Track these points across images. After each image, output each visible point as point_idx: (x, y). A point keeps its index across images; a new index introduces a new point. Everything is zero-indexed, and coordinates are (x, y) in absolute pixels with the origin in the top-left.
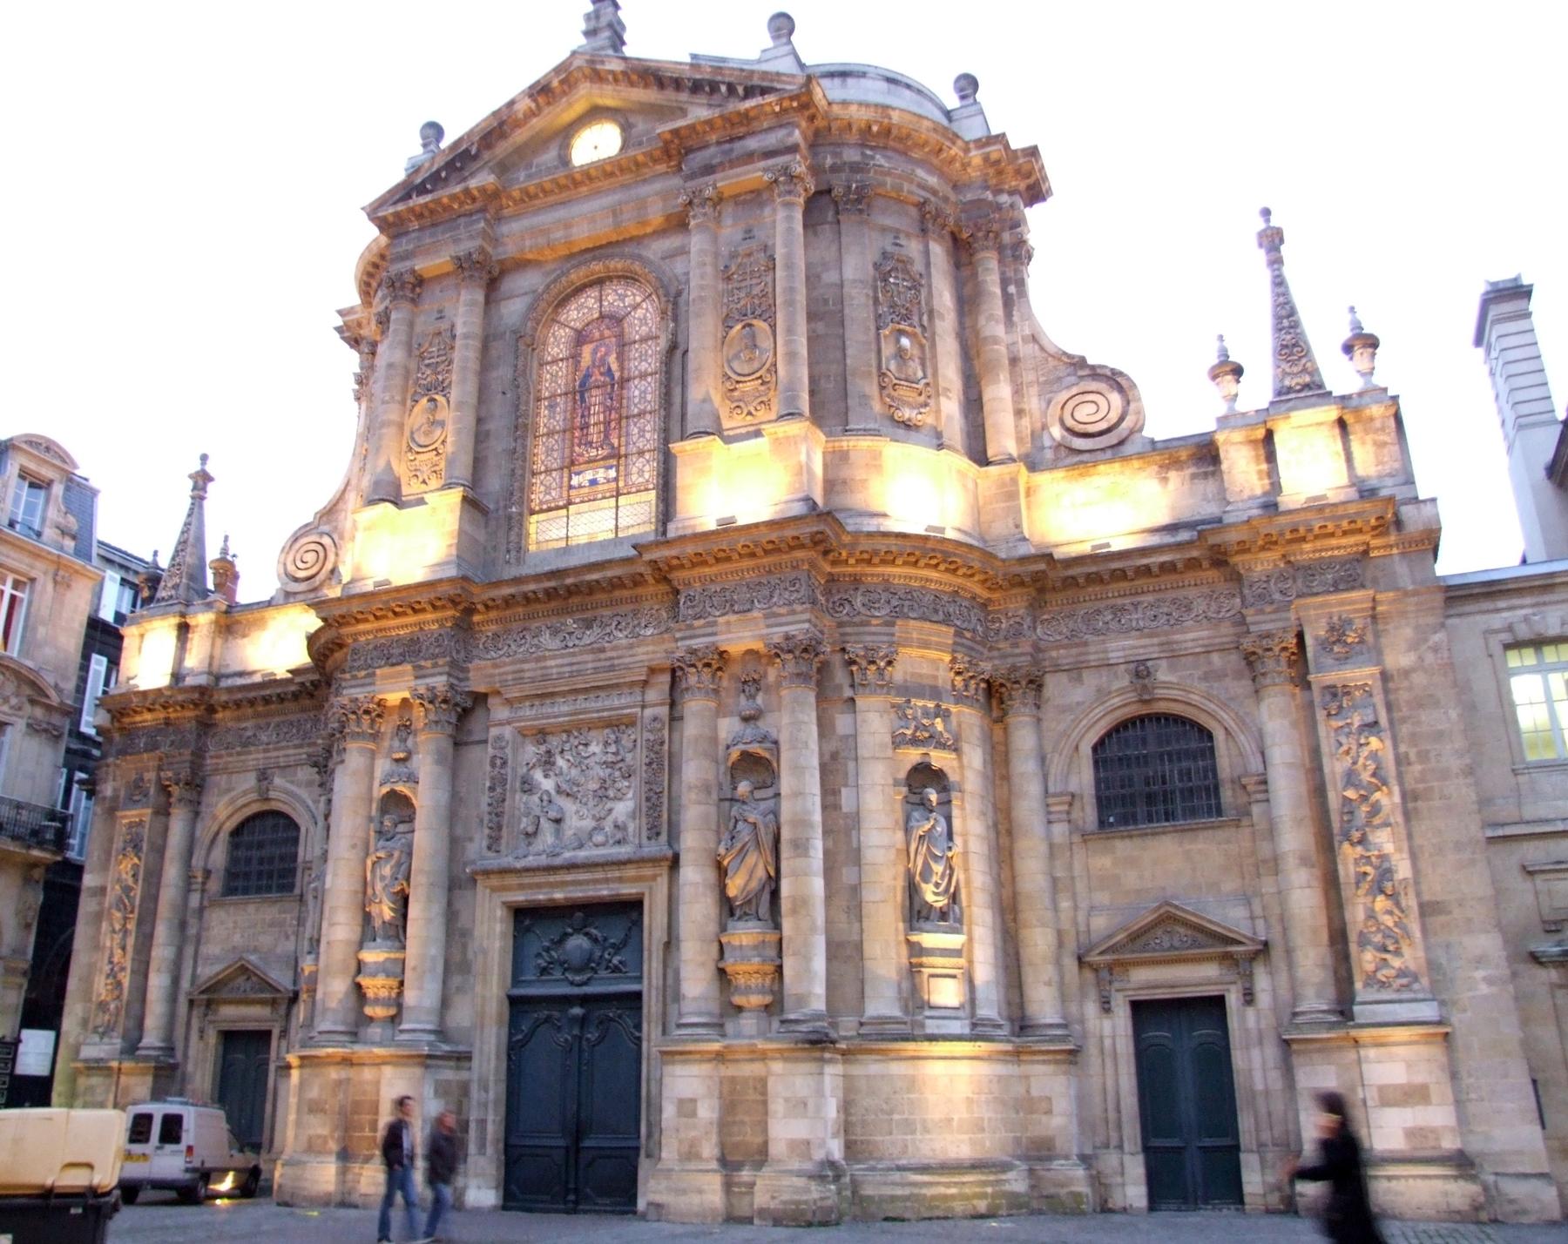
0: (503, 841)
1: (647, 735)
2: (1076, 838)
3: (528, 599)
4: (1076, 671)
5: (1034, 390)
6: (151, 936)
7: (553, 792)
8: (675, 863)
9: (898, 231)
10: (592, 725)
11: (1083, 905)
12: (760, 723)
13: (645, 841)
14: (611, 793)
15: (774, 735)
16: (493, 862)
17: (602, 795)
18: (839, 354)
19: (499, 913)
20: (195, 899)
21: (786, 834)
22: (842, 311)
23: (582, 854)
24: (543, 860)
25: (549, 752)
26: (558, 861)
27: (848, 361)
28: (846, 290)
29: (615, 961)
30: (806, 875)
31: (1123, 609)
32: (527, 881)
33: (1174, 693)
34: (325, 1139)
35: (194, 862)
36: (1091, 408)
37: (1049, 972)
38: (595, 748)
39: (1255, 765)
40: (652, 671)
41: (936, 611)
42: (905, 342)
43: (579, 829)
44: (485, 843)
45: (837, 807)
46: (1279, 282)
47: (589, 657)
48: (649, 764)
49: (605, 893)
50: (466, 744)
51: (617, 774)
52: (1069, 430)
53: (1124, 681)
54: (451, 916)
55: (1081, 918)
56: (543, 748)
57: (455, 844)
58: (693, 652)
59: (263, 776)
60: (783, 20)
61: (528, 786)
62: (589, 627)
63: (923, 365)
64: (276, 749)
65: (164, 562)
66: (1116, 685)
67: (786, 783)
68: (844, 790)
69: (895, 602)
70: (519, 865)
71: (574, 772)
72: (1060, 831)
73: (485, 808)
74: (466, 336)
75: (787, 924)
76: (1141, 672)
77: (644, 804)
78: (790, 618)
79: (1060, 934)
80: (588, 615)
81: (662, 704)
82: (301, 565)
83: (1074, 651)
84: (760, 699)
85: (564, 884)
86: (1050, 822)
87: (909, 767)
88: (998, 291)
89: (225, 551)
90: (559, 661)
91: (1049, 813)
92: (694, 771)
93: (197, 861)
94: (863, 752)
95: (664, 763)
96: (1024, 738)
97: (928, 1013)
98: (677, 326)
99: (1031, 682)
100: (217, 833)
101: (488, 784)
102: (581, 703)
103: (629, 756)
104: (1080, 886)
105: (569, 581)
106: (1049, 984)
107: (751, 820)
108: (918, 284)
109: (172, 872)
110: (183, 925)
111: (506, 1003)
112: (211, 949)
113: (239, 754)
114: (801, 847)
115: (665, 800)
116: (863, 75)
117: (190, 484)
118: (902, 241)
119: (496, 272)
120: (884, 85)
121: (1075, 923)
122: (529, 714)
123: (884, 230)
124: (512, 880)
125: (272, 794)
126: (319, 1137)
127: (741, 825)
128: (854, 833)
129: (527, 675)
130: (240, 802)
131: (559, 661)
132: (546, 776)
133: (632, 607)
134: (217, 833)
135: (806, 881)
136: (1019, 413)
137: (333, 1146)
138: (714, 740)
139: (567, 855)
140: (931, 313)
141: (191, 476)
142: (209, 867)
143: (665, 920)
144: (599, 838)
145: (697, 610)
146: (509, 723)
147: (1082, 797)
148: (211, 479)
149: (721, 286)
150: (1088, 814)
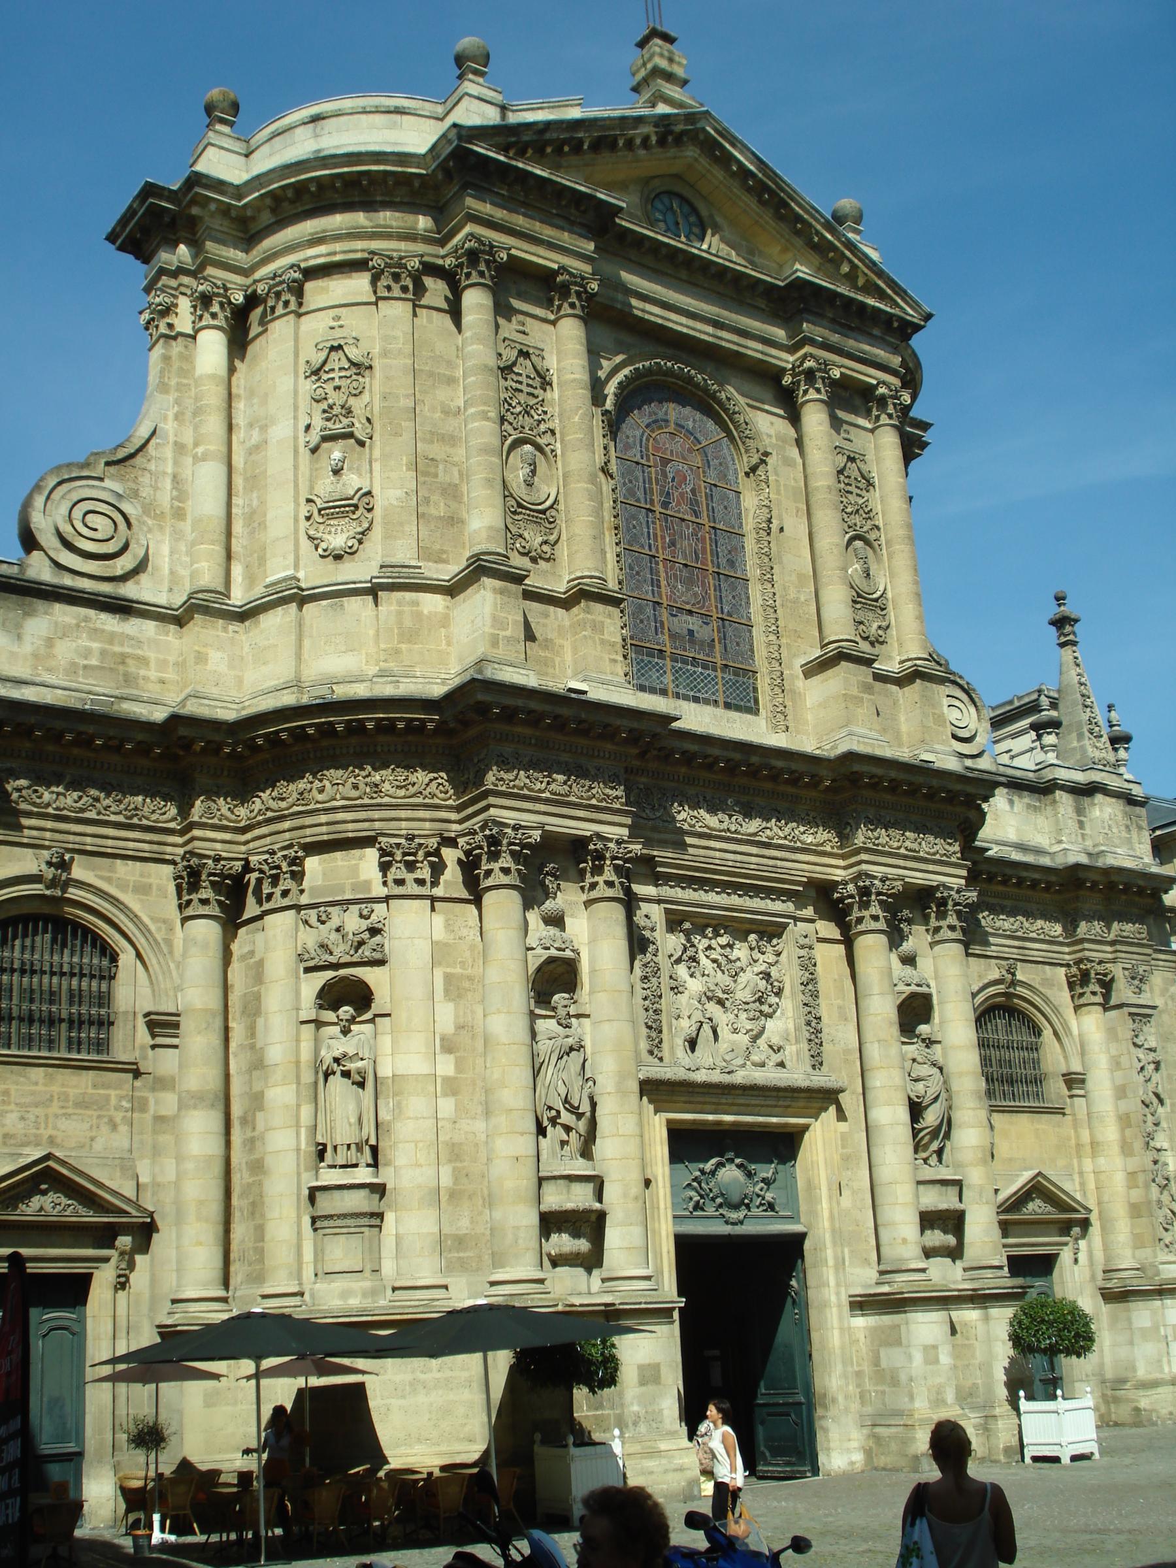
0: (665, 1045)
29: (769, 1196)
36: (959, 716)
146: (659, 902)
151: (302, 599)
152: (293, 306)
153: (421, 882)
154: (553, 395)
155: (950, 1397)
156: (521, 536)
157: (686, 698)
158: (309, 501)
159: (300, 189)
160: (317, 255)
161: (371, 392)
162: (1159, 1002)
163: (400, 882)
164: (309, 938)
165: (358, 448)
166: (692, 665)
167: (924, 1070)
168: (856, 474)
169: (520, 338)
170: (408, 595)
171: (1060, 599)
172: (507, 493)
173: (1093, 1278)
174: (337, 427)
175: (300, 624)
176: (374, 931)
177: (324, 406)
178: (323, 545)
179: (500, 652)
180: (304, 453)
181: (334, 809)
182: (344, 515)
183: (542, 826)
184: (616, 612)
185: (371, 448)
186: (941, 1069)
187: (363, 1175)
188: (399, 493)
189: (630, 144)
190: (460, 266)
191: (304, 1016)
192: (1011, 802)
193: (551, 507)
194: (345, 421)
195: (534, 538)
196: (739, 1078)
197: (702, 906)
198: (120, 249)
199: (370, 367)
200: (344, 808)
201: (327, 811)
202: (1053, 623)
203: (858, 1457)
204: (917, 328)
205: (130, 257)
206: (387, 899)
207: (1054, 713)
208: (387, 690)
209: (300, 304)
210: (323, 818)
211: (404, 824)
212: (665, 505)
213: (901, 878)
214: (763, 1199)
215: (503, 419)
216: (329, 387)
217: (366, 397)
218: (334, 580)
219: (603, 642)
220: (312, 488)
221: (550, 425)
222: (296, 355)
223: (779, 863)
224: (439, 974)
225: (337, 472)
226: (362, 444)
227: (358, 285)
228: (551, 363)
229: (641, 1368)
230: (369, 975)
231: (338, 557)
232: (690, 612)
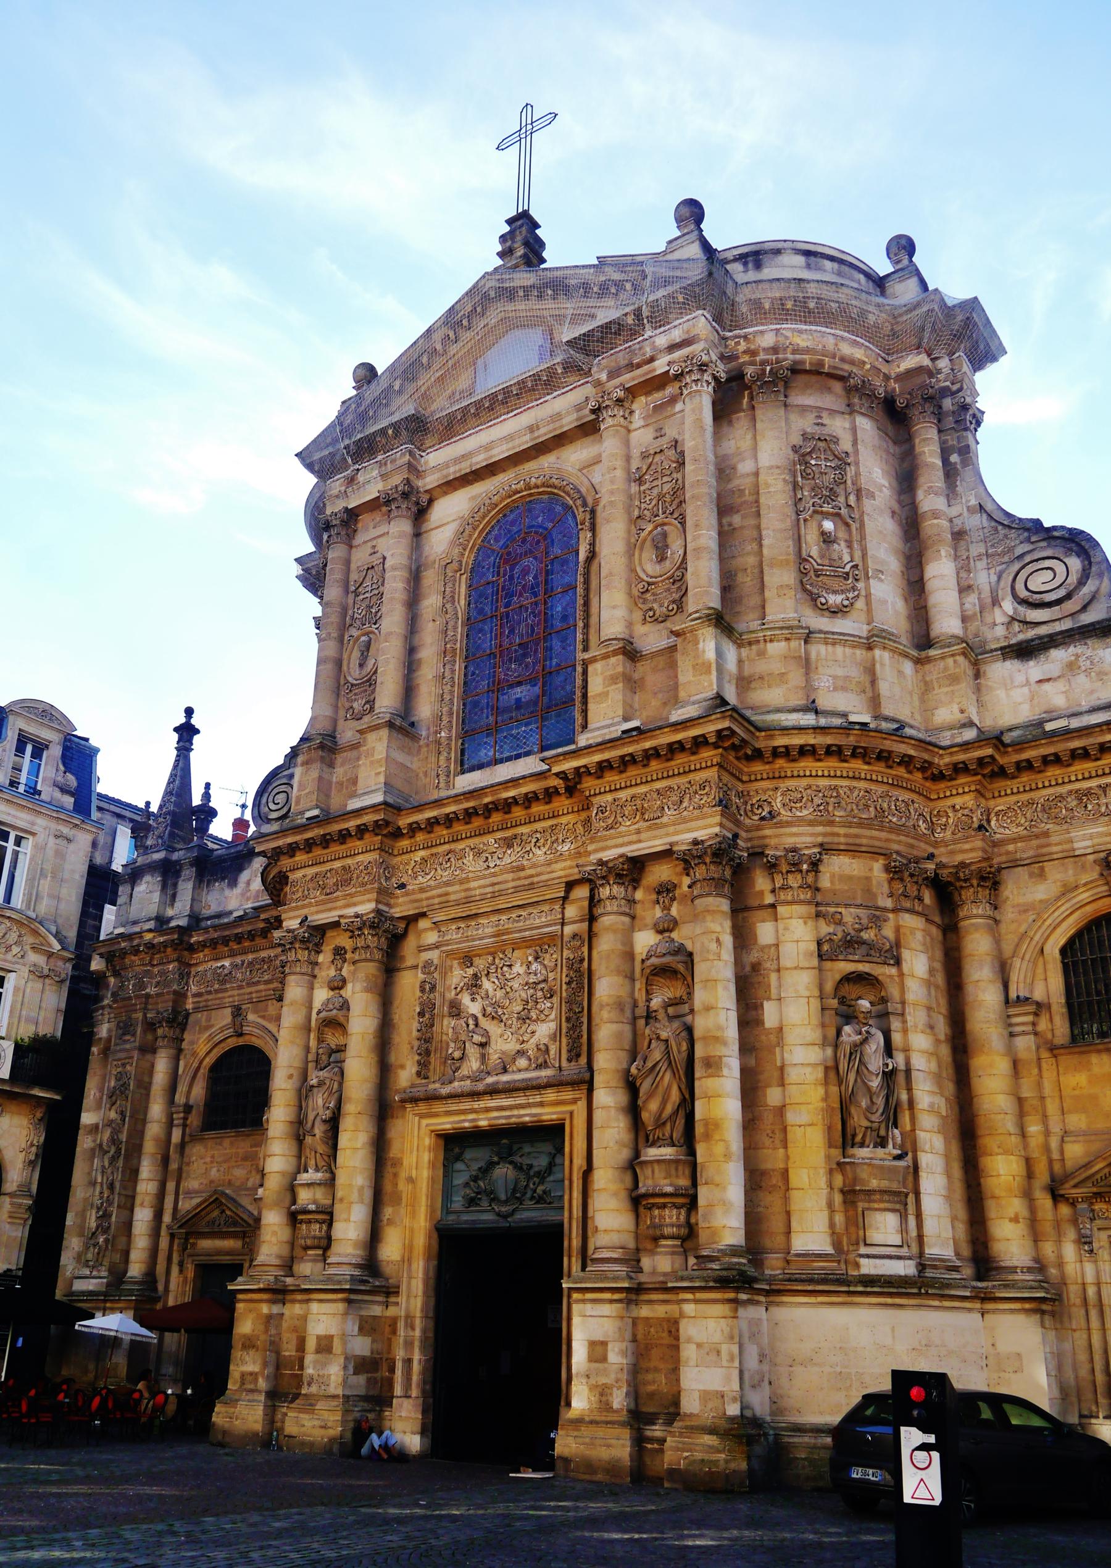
0: (431, 1068)
2: (1045, 1054)
3: (449, 821)
4: (1037, 865)
5: (981, 564)
6: (136, 1172)
7: (480, 1016)
8: (587, 1084)
9: (820, 409)
11: (1056, 1128)
12: (674, 935)
13: (564, 1064)
15: (689, 948)
16: (419, 1092)
17: (524, 1019)
18: (755, 546)
19: (427, 1141)
20: (176, 1135)
21: (699, 1052)
22: (757, 501)
23: (505, 1078)
24: (467, 1085)
25: (475, 976)
26: (480, 1087)
27: (765, 551)
28: (761, 478)
30: (719, 1096)
31: (1088, 793)
35: (177, 1097)
37: (1016, 1205)
38: (518, 968)
40: (570, 886)
41: (867, 806)
42: (828, 525)
43: (503, 1053)
44: (414, 1070)
45: (759, 1022)
47: (510, 876)
48: (568, 983)
49: (527, 1119)
50: (398, 970)
51: (540, 994)
52: (1024, 602)
54: (380, 1147)
55: (1054, 1143)
56: (470, 971)
57: (384, 1069)
58: (601, 863)
59: (237, 1012)
60: (686, 211)
61: (455, 1009)
62: (510, 846)
63: (850, 546)
64: (249, 985)
65: (154, 808)
66: (1085, 878)
67: (700, 996)
68: (766, 1005)
69: (817, 801)
70: (445, 1090)
71: (500, 994)
72: (1025, 1044)
73: (415, 1034)
74: (394, 569)
75: (700, 1149)
77: (564, 1024)
78: (700, 823)
79: (1028, 1162)
80: (508, 834)
81: (582, 921)
82: (273, 807)
83: (1035, 843)
84: (674, 911)
85: (488, 1110)
86: (1012, 1035)
87: (838, 977)
88: (939, 462)
89: (207, 796)
90: (482, 882)
91: (1010, 1025)
92: (607, 987)
93: (180, 1099)
94: (785, 962)
95: (581, 979)
96: (978, 945)
97: (863, 1250)
98: (594, 536)
99: (983, 879)
100: (198, 1068)
101: (418, 1010)
103: (551, 976)
104: (1052, 1107)
105: (487, 800)
106: (1015, 1220)
107: (663, 1037)
108: (842, 462)
109: (156, 1109)
110: (165, 1160)
111: (435, 1236)
112: (192, 1183)
113: (217, 991)
114: (713, 1065)
115: (585, 1020)
116: (778, 252)
117: (176, 736)
118: (825, 421)
119: (425, 498)
120: (800, 260)
121: (1047, 1149)
123: (804, 409)
125: (246, 1029)
127: (654, 1044)
128: (777, 1049)
129: (452, 897)
130: (217, 1039)
131: (482, 882)
132: (473, 1000)
133: (550, 823)
134: (198, 1068)
135: (721, 1101)
136: (964, 589)
138: (630, 955)
139: (490, 1080)
140: (859, 493)
141: (176, 730)
142: (191, 1102)
143: (585, 1146)
145: (610, 821)
146: (437, 947)
147: (1049, 1006)
148: (197, 732)
149: (634, 488)
150: (1059, 1026)
157: (509, 759)
166: (517, 727)
197: (474, 940)
212: (507, 605)
214: (535, 1191)
219: (372, 763)
223: (535, 879)
232: (519, 684)
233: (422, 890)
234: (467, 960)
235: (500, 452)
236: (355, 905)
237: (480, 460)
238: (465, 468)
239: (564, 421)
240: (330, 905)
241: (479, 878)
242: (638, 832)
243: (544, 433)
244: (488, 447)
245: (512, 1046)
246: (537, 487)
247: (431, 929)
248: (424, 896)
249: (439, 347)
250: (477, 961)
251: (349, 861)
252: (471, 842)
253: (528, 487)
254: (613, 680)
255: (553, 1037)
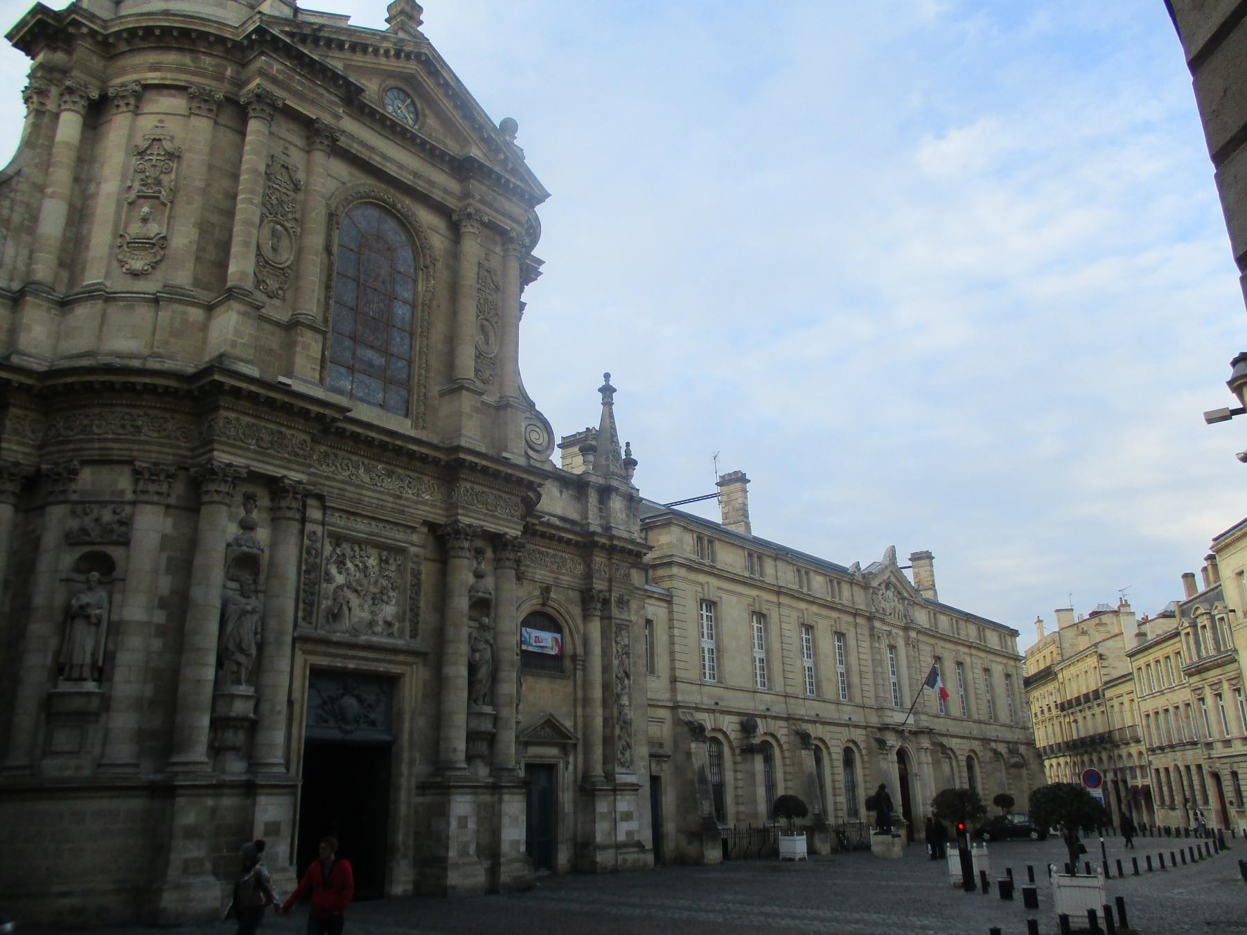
0: (314, 615)
1: (411, 565)
10: (376, 545)
13: (407, 637)
14: (385, 598)
17: (378, 599)
23: (375, 639)
24: (346, 638)
32: (333, 650)
33: (556, 606)
34: (201, 862)
39: (580, 651)
40: (425, 523)
44: (300, 614)
46: (611, 416)
47: (391, 499)
53: (537, 593)
56: (338, 551)
58: (470, 526)
61: (329, 579)
62: (389, 477)
71: (358, 575)
76: (546, 590)
85: (354, 658)
101: (304, 568)
102: (374, 527)
105: (398, 443)
122: (338, 522)
124: (322, 649)
126: (194, 859)
137: (208, 866)
144: (379, 629)
151: (110, 298)
152: (131, 108)
153: (158, 493)
154: (300, 197)
155: (472, 849)
156: (264, 281)
158: (121, 236)
159: (149, 31)
160: (153, 77)
161: (177, 173)
162: (634, 618)
163: (144, 492)
164: (74, 524)
165: (161, 207)
167: (482, 645)
168: (489, 281)
169: (283, 157)
170: (181, 308)
171: (607, 376)
172: (259, 254)
173: (575, 781)
174: (149, 192)
175: (104, 315)
176: (121, 523)
177: (142, 176)
178: (127, 266)
179: (237, 352)
180: (126, 205)
181: (106, 440)
182: (145, 249)
183: (248, 467)
184: (319, 337)
185: (172, 208)
186: (491, 646)
187: (91, 686)
188: (185, 241)
189: (376, 52)
190: (249, 103)
191: (64, 575)
192: (561, 492)
193: (288, 267)
194: (156, 189)
195: (273, 284)
196: (363, 638)
198: (16, 45)
199: (179, 157)
200: (114, 440)
201: (100, 440)
202: (600, 390)
203: (410, 887)
204: (540, 201)
205: (22, 54)
206: (134, 503)
207: (594, 443)
208: (154, 365)
209: (137, 107)
210: (97, 445)
211: (154, 455)
213: (481, 527)
215: (264, 205)
216: (147, 165)
217: (173, 176)
218: (130, 289)
220: (126, 227)
221: (297, 216)
222: (130, 137)
224: (164, 556)
225: (145, 220)
226: (165, 205)
227: (176, 103)
228: (301, 176)
229: (267, 825)
230: (116, 553)
231: (136, 275)
233: (327, 478)
234: (338, 540)
235: (392, 170)
236: (290, 469)
237: (376, 160)
238: (365, 154)
239: (436, 191)
240: (267, 459)
241: (368, 489)
242: (486, 515)
243: (421, 186)
244: (385, 157)
245: (366, 615)
246: (398, 211)
247: (317, 508)
248: (327, 483)
249: (382, 51)
250: (344, 545)
251: (284, 430)
252: (366, 461)
253: (394, 206)
254: (477, 410)
255: (400, 617)
